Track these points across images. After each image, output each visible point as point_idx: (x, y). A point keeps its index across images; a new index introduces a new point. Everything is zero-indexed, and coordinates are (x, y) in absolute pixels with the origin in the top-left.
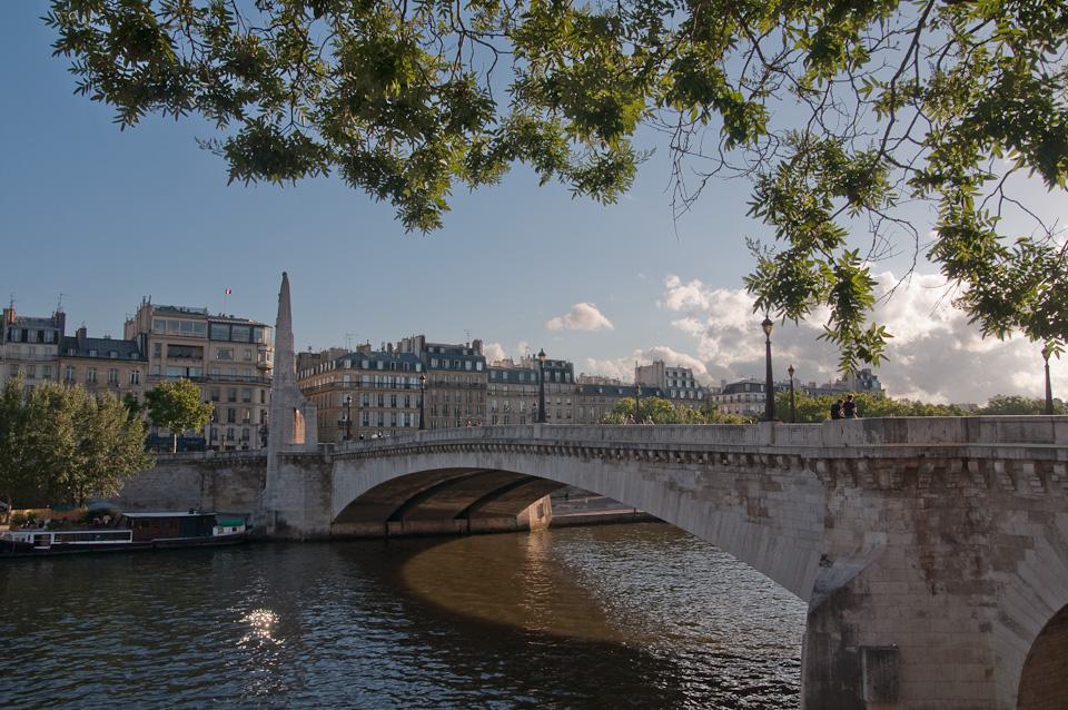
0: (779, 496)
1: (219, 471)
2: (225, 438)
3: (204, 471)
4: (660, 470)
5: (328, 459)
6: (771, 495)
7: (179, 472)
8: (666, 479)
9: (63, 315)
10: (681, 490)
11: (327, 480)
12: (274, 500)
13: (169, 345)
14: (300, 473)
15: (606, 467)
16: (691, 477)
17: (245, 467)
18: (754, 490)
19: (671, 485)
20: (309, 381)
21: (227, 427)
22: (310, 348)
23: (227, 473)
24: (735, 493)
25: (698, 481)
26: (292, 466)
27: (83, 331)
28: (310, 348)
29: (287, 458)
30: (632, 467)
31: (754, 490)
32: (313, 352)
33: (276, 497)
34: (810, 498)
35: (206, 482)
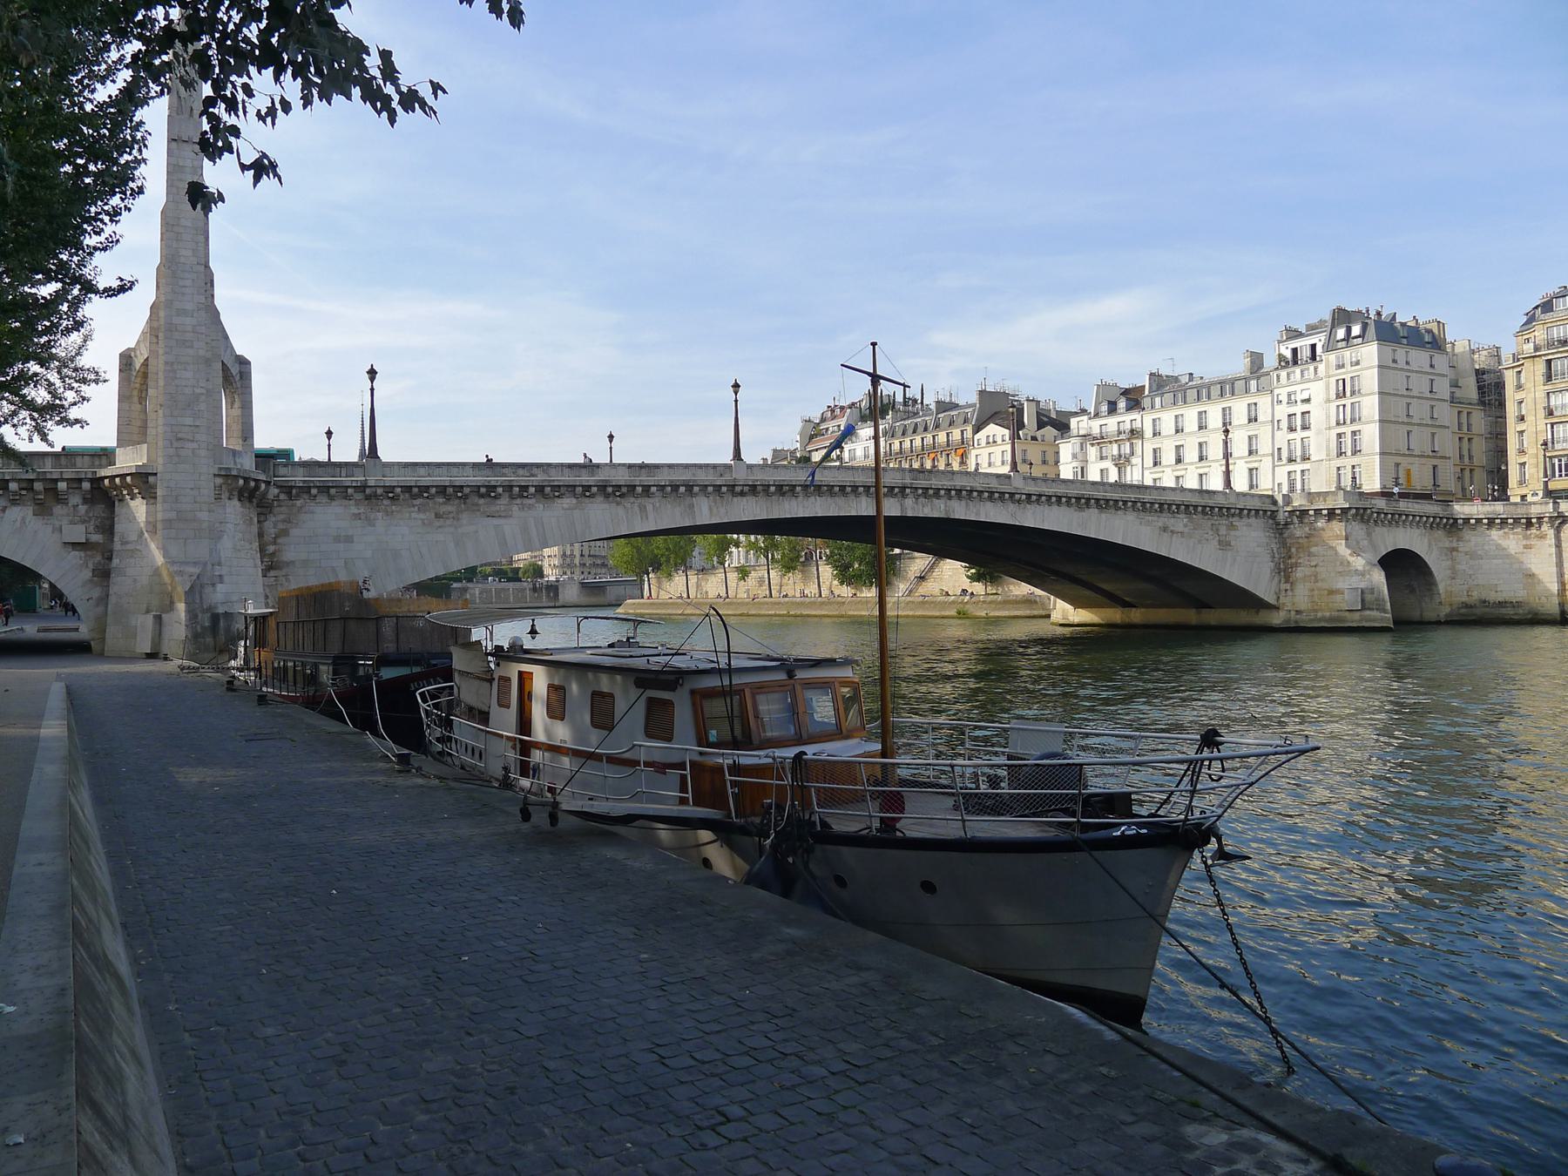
0: (1237, 533)
4: (1156, 518)
6: (1232, 533)
8: (1160, 524)
10: (1172, 531)
12: (219, 587)
15: (1103, 515)
16: (1180, 523)
18: (1223, 531)
19: (1165, 529)
24: (1211, 533)
25: (1185, 526)
26: (236, 502)
30: (1131, 517)
31: (1223, 531)
34: (1254, 534)
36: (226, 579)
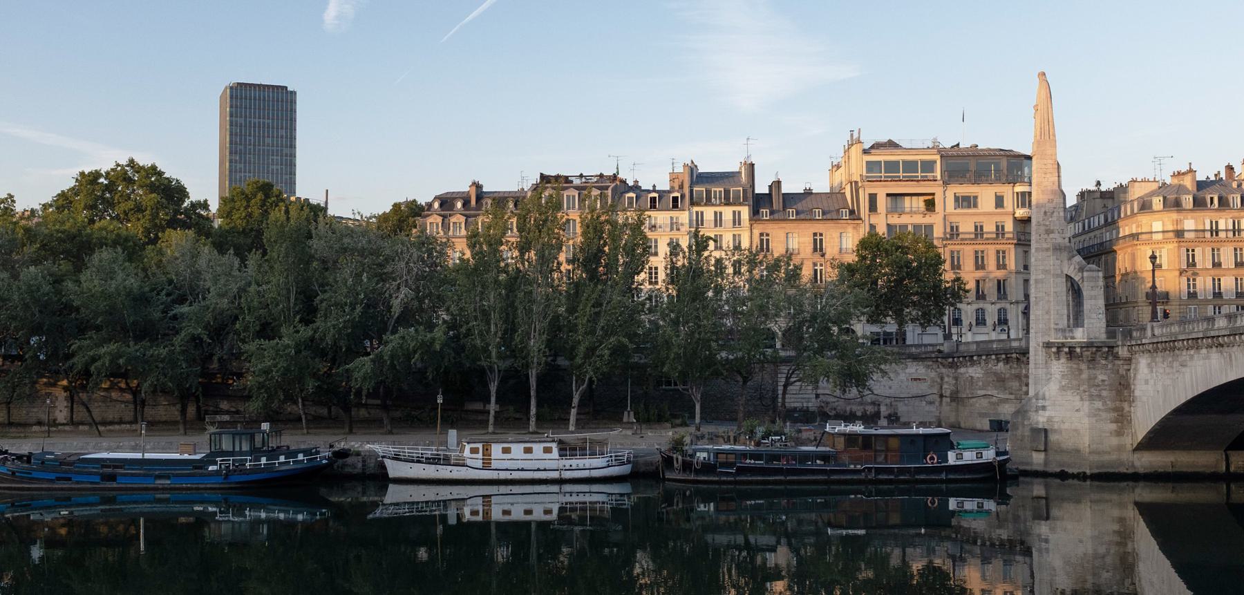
1: (962, 370)
2: (974, 323)
3: (944, 370)
5: (1123, 352)
7: (907, 371)
9: (752, 165)
11: (1123, 388)
13: (888, 195)
14: (1080, 371)
17: (1001, 364)
20: (1097, 233)
21: (975, 306)
22: (1098, 183)
23: (975, 372)
26: (1063, 360)
27: (777, 184)
28: (1098, 183)
29: (1060, 347)
32: (1103, 188)
33: (1044, 408)
35: (945, 386)
36: (1048, 408)
